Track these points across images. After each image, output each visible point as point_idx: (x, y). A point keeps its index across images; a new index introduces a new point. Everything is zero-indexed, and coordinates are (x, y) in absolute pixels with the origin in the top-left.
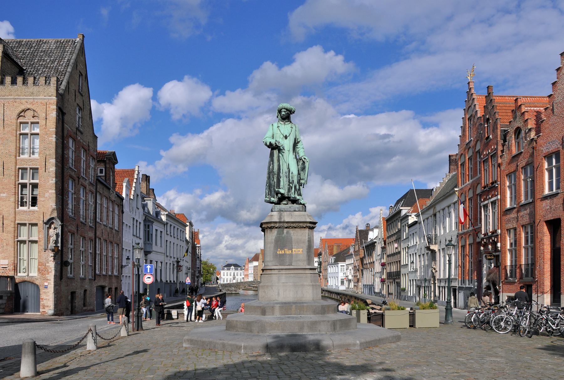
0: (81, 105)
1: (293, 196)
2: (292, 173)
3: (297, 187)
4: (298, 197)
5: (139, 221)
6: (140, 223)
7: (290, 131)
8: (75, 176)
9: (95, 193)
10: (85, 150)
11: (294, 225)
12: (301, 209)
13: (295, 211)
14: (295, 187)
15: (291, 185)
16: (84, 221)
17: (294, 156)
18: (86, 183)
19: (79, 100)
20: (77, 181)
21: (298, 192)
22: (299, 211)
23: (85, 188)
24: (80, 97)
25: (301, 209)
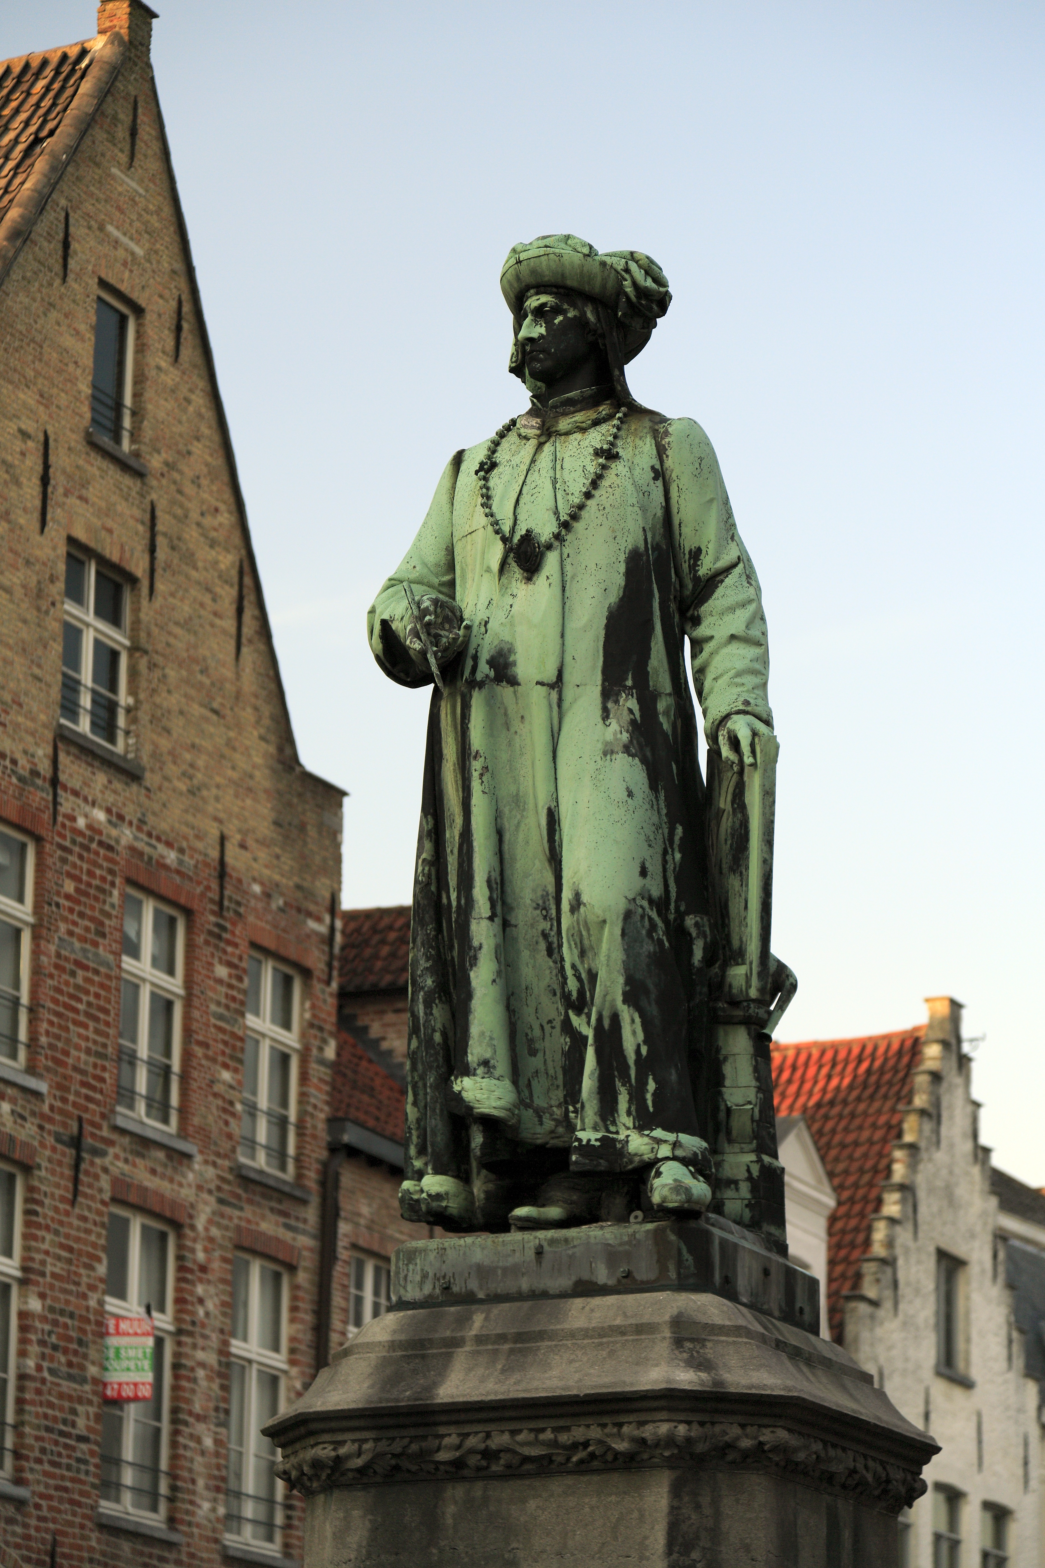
0: (125, 545)
1: (588, 1135)
2: (577, 904)
3: (632, 1037)
4: (638, 1144)
5: (977, 1492)
6: (999, 1514)
7: (577, 485)
8: (27, 1132)
9: (308, 1262)
10: (177, 911)
11: (526, 1441)
12: (645, 1271)
13: (586, 1289)
14: (609, 1037)
15: (577, 1021)
16: (153, 1521)
17: (616, 731)
18: (193, 1188)
19: (103, 512)
20: (51, 1179)
21: (637, 1096)
22: (628, 1284)
23: (168, 1224)
24: (105, 481)
25: (645, 1271)
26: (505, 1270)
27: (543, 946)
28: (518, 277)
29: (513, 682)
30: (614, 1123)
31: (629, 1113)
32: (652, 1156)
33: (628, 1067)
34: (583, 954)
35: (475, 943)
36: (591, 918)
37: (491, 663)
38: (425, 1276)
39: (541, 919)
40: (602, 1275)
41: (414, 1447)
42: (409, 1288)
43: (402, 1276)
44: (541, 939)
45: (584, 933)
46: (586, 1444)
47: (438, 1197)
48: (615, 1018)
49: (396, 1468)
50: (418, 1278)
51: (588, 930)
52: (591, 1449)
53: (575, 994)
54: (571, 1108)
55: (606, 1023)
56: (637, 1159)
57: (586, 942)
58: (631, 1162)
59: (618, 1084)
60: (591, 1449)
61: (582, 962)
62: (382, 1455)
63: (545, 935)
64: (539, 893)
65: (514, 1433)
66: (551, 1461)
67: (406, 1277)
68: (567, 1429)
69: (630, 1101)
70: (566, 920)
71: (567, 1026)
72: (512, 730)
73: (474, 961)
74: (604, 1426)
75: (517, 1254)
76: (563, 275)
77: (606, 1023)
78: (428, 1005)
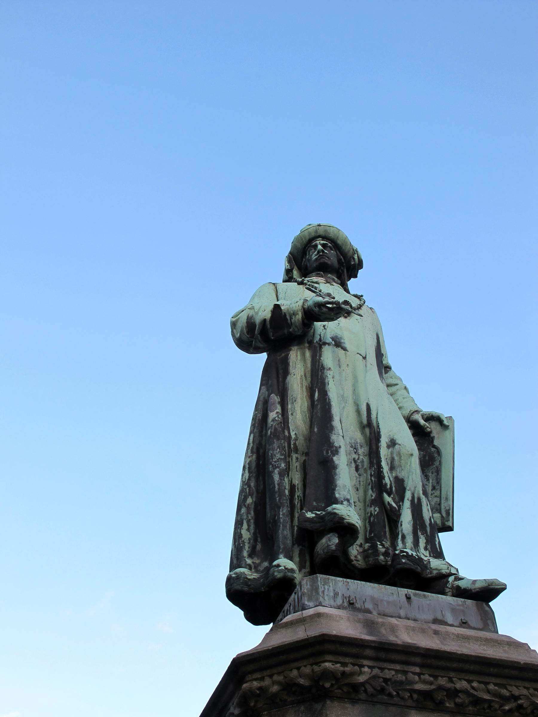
2: (392, 443)
26: (388, 603)
27: (353, 465)
28: (316, 231)
29: (345, 349)
30: (418, 551)
31: (426, 549)
32: (448, 571)
33: (426, 526)
34: (392, 468)
35: (336, 444)
36: (403, 451)
37: (333, 339)
38: (336, 594)
39: (353, 452)
40: (450, 619)
41: (401, 677)
42: (326, 598)
43: (321, 590)
44: (353, 462)
45: (396, 458)
46: (516, 698)
47: (292, 570)
48: (419, 499)
49: (382, 690)
50: (332, 594)
51: (400, 457)
52: (520, 702)
53: (388, 486)
54: (379, 543)
55: (416, 500)
56: (435, 572)
57: (396, 463)
58: (431, 573)
59: (419, 533)
60: (520, 702)
61: (391, 473)
62: (375, 677)
63: (355, 461)
64: (353, 441)
65: (469, 682)
66: (490, 707)
67: (323, 592)
68: (504, 686)
69: (427, 543)
70: (384, 452)
71: (379, 501)
72: (342, 368)
73: (336, 452)
74: (528, 689)
75: (395, 596)
76: (338, 237)
77: (416, 500)
78: (281, 474)
